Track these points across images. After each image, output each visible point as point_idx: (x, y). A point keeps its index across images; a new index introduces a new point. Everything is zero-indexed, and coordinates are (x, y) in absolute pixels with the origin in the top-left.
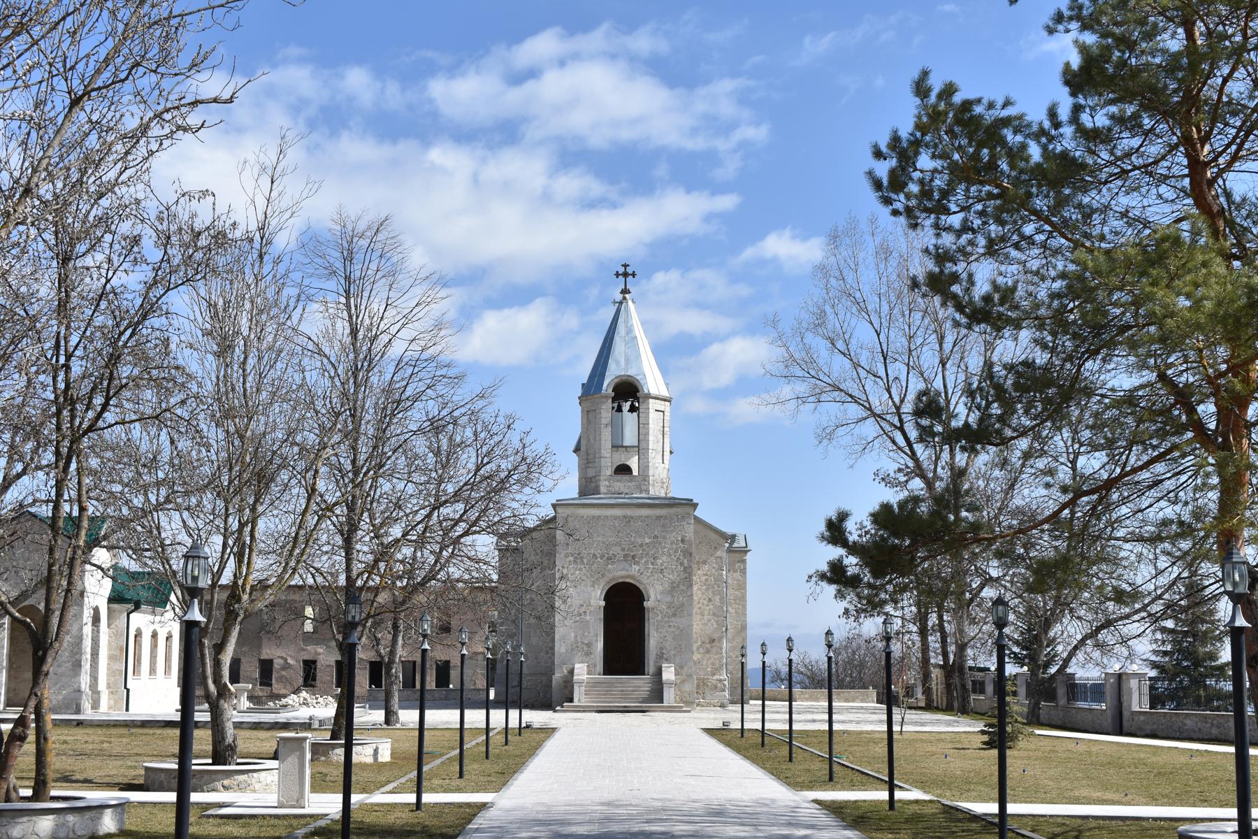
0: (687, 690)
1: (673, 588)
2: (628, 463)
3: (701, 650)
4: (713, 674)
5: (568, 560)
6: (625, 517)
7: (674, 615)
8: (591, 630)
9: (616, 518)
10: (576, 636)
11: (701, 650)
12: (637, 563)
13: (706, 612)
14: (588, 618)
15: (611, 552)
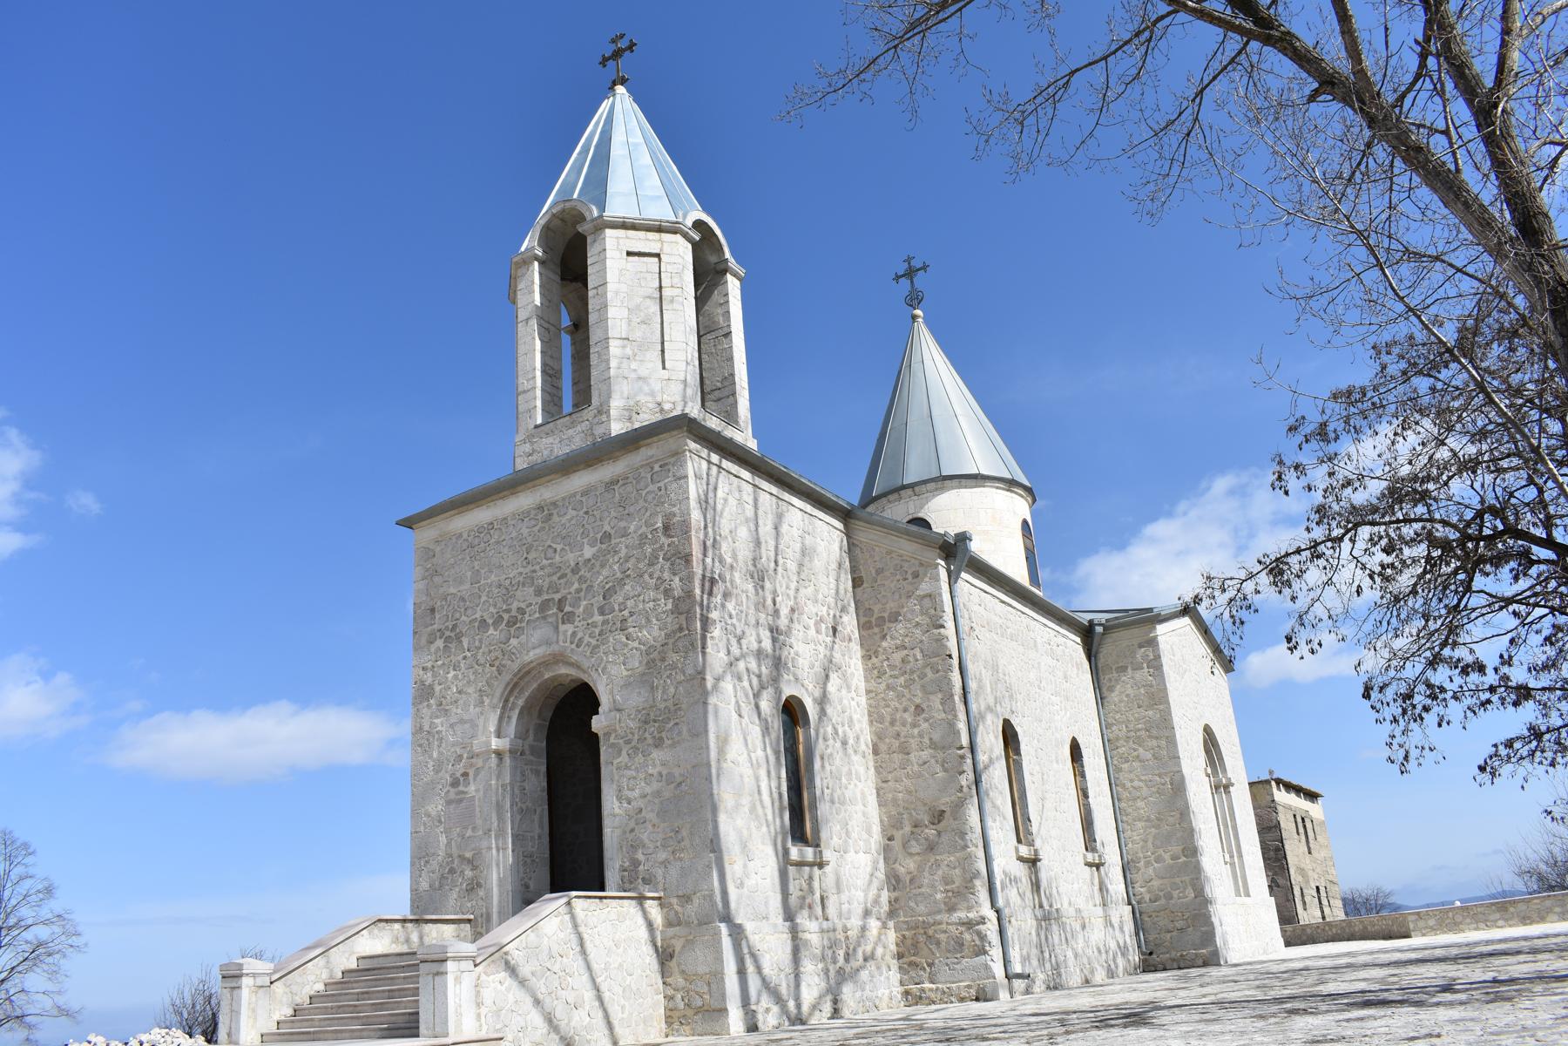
0: (702, 969)
1: (651, 664)
2: (921, 515)
3: (915, 848)
4: (952, 909)
5: (433, 648)
6: (540, 508)
7: (658, 743)
8: (479, 822)
9: (523, 516)
10: (449, 844)
11: (915, 848)
12: (569, 618)
13: (913, 743)
15: (515, 606)
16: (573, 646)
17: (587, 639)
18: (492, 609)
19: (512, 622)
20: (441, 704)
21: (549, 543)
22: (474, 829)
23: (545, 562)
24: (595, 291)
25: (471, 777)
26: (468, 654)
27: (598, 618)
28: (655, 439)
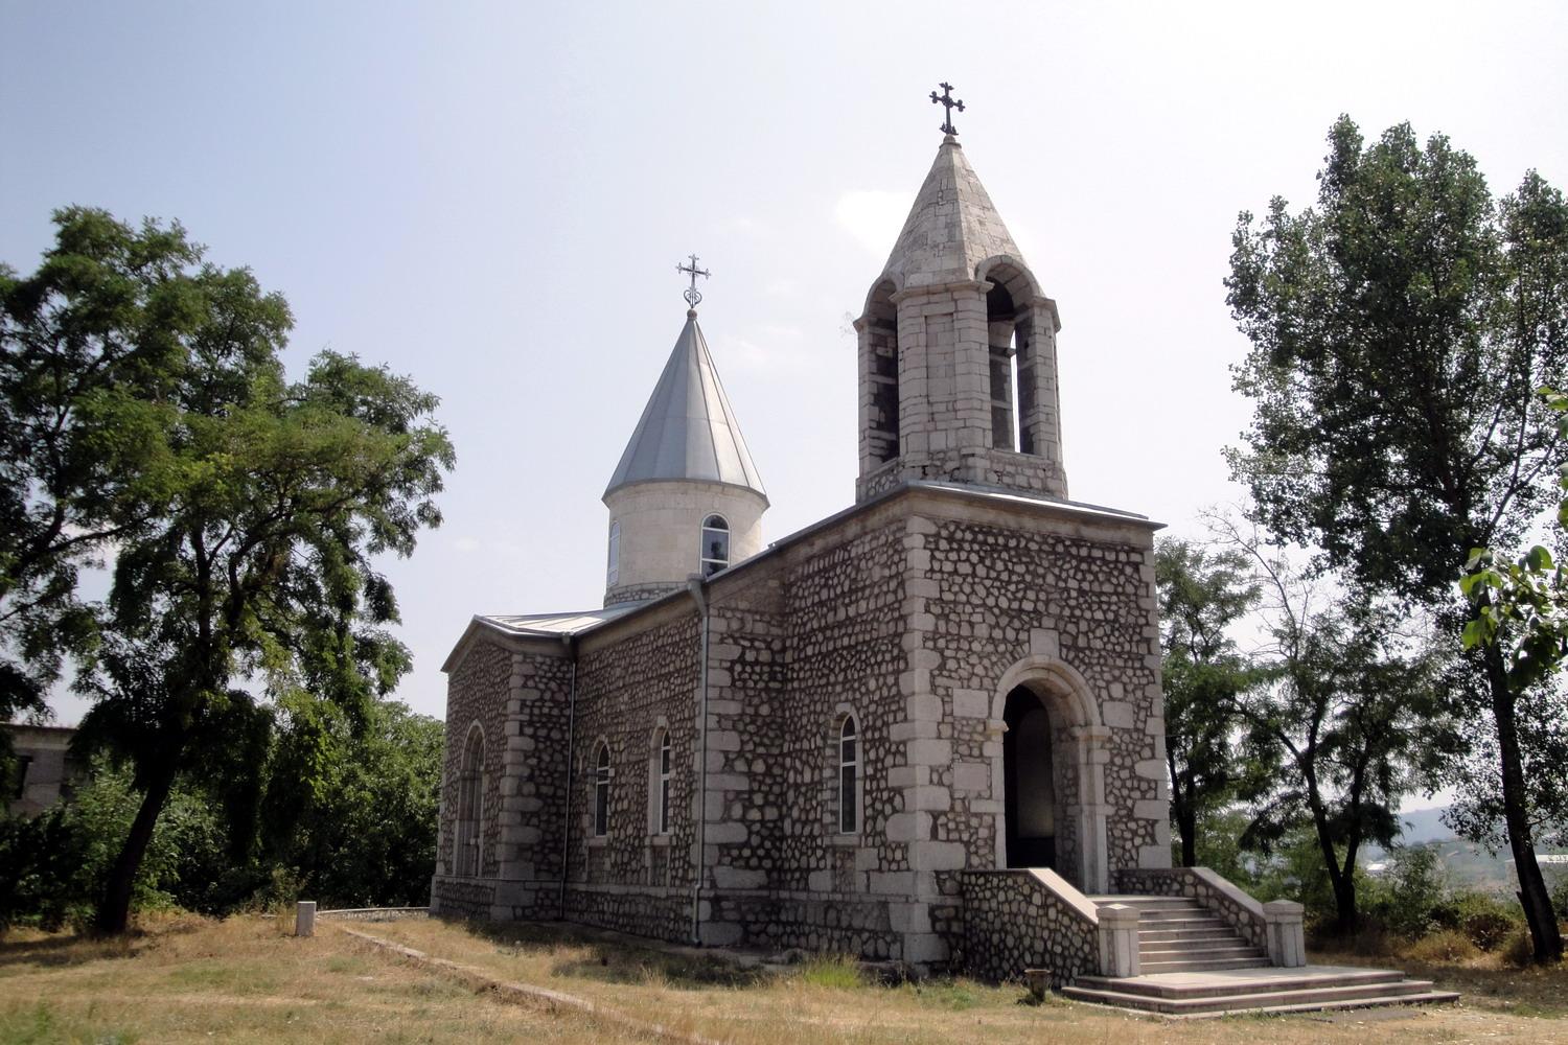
24: (1042, 360)
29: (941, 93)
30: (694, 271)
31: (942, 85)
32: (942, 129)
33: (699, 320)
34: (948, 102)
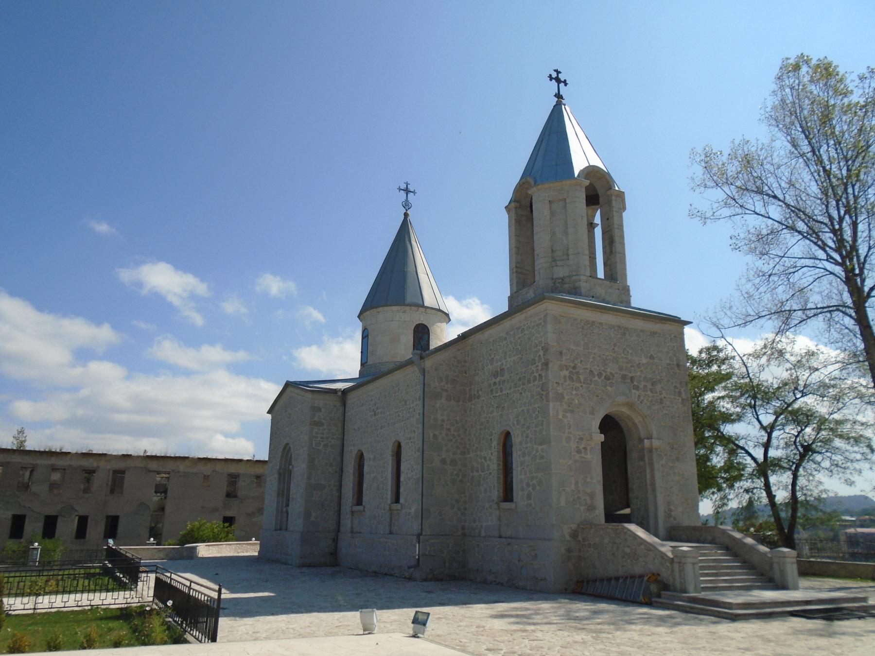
6: (619, 327)
7: (678, 459)
10: (576, 483)
12: (636, 388)
14: (589, 456)
15: (609, 370)
16: (639, 402)
17: (645, 401)
18: (596, 367)
19: (607, 378)
20: (569, 406)
21: (624, 347)
22: (591, 478)
23: (623, 355)
25: (588, 451)
26: (584, 386)
27: (649, 393)
28: (673, 323)
29: (554, 75)
30: (407, 191)
31: (555, 70)
32: (555, 96)
33: (410, 218)
34: (558, 80)
